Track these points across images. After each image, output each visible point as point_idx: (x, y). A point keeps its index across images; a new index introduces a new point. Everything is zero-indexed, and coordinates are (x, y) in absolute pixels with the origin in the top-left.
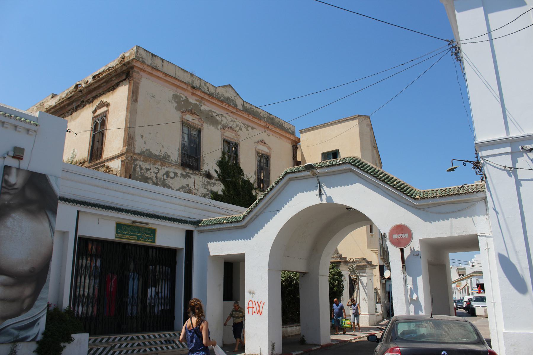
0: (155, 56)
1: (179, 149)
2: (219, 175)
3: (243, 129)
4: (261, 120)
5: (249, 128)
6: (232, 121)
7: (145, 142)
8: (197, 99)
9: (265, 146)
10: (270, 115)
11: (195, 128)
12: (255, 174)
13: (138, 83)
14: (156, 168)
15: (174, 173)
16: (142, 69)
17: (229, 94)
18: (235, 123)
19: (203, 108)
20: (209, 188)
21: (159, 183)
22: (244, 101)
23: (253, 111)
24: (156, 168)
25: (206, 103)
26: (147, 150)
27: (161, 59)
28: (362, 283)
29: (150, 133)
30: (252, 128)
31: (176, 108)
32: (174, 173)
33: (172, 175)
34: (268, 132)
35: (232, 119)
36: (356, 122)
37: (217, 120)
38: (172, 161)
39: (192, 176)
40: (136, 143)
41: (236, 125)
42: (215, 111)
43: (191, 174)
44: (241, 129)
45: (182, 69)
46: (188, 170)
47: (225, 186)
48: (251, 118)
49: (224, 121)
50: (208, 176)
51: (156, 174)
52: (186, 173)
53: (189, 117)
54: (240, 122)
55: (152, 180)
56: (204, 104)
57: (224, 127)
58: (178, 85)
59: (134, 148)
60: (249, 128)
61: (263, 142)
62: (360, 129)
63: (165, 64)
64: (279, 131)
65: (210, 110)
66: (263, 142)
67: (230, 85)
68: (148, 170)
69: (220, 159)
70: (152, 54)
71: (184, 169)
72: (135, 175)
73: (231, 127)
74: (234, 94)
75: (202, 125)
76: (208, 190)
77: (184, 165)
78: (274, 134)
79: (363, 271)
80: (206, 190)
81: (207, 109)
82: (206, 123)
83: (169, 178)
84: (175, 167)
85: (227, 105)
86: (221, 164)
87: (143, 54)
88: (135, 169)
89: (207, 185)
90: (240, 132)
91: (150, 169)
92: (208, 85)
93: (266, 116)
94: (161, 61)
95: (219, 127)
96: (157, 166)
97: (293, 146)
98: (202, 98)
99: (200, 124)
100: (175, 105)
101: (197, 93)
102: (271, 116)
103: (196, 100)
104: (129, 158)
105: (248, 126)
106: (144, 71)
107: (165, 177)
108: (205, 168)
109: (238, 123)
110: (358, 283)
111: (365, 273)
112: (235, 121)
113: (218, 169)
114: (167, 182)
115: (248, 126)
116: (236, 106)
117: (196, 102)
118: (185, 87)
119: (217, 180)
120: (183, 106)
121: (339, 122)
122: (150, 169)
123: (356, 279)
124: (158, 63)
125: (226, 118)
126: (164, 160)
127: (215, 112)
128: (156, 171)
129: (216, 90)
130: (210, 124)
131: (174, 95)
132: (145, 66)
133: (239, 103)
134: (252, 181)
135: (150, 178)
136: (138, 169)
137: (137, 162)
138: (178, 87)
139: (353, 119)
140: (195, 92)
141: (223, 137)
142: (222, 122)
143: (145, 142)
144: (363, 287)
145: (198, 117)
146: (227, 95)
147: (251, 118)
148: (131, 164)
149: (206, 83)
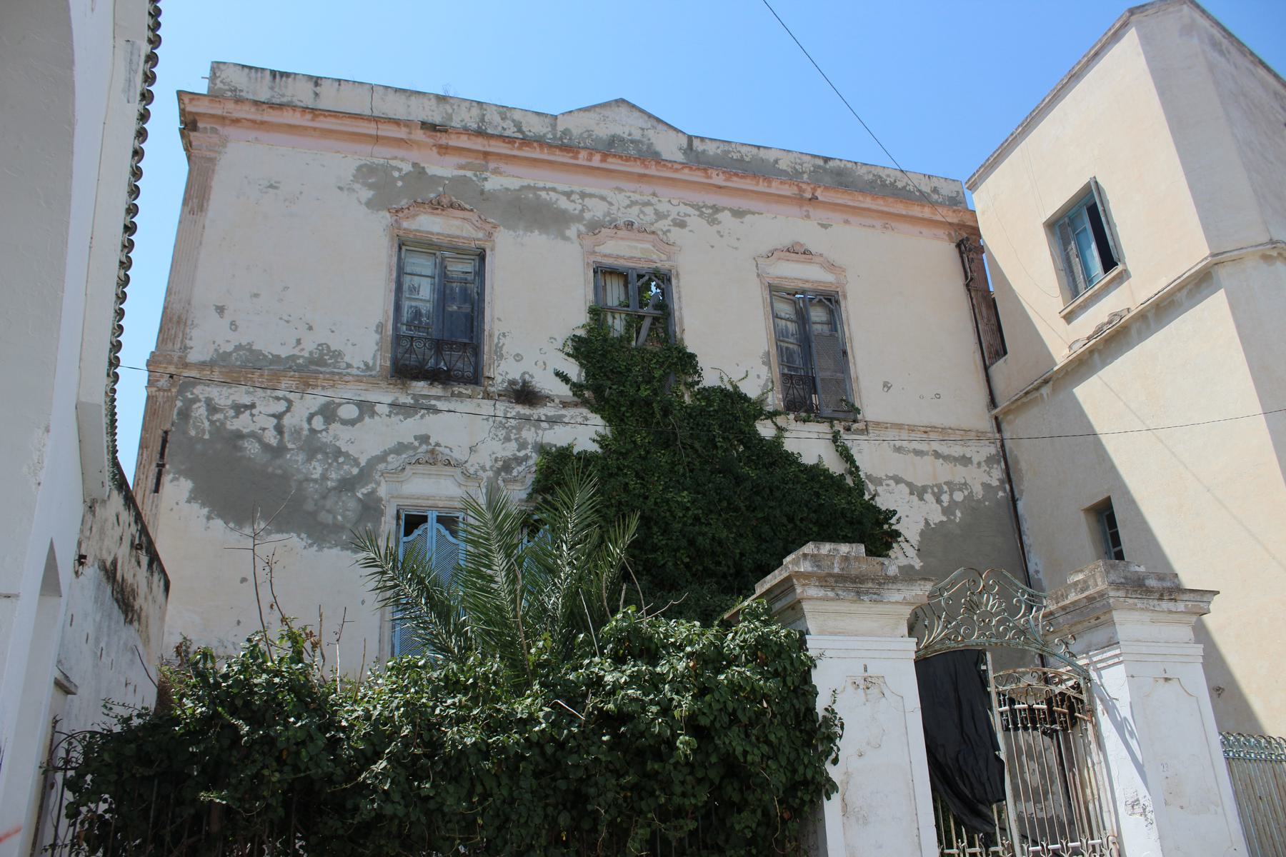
0: (287, 75)
1: (380, 328)
2: (577, 388)
3: (694, 221)
4: (768, 180)
5: (725, 216)
6: (633, 203)
7: (233, 323)
8: (463, 161)
9: (810, 262)
10: (826, 160)
11: (460, 252)
12: (767, 363)
13: (212, 161)
14: (278, 398)
15: (361, 405)
16: (223, 118)
17: (625, 125)
18: (649, 210)
19: (493, 183)
20: (529, 435)
21: (290, 446)
22: (690, 138)
23: (741, 160)
24: (278, 398)
25: (503, 167)
26: (239, 347)
27: (310, 77)
28: (1110, 709)
29: (256, 295)
30: (738, 214)
31: (369, 204)
32: (361, 405)
33: (349, 412)
34: (819, 214)
35: (635, 197)
36: (1131, 38)
37: (564, 212)
38: (349, 366)
39: (440, 405)
40: (195, 333)
41: (657, 213)
42: (549, 185)
43: (438, 398)
44: (682, 225)
45: (397, 90)
46: (420, 387)
47: (609, 421)
48: (719, 180)
49: (597, 210)
50: (525, 394)
51: (279, 416)
52: (415, 397)
53: (431, 224)
54: (671, 202)
55: (259, 439)
56: (496, 172)
57: (595, 227)
58: (374, 132)
59: (185, 348)
60: (725, 216)
61: (798, 252)
62: (1149, 61)
63: (324, 89)
64: (879, 205)
65: (523, 188)
66: (798, 252)
67: (623, 101)
68: (239, 409)
69: (582, 333)
70: (273, 73)
71: (404, 388)
72: (185, 433)
73: (630, 225)
74: (642, 122)
75: (490, 235)
76: (522, 446)
77: (403, 371)
78: (852, 219)
79: (1100, 636)
80: (514, 445)
81: (513, 183)
82: (509, 228)
83: (335, 426)
84: (363, 386)
85: (597, 157)
86: (590, 348)
87: (240, 80)
88: (185, 414)
89: (519, 429)
90: (676, 234)
91: (253, 406)
92: (517, 116)
93: (808, 166)
94: (310, 85)
95: (572, 232)
96: (280, 394)
97: (958, 246)
98: (486, 155)
99: (481, 235)
100: (367, 194)
101: (451, 143)
102: (831, 164)
103: (461, 167)
104: (164, 382)
105: (716, 209)
106: (236, 121)
107: (318, 423)
108: (504, 371)
109: (663, 207)
110: (1092, 712)
111: (1112, 643)
112: (648, 204)
113: (574, 370)
114: (325, 438)
115: (716, 209)
116: (656, 158)
117: (462, 172)
118: (401, 133)
119: (565, 405)
120: (385, 191)
121: (1074, 77)
122: (253, 406)
123: (1077, 687)
124: (303, 94)
125: (603, 198)
126: (312, 370)
127: (554, 190)
128: (281, 406)
129: (554, 126)
130: (529, 228)
131: (359, 169)
132: (230, 106)
133: (669, 148)
134: (751, 390)
135: (253, 435)
136: (200, 411)
137: (198, 390)
138: (377, 139)
139: (1116, 36)
141: (592, 259)
142: (587, 215)
143: (233, 323)
144: (1120, 726)
145: (467, 215)
146: (603, 131)
147: (719, 180)
148: (172, 401)
149: (504, 111)
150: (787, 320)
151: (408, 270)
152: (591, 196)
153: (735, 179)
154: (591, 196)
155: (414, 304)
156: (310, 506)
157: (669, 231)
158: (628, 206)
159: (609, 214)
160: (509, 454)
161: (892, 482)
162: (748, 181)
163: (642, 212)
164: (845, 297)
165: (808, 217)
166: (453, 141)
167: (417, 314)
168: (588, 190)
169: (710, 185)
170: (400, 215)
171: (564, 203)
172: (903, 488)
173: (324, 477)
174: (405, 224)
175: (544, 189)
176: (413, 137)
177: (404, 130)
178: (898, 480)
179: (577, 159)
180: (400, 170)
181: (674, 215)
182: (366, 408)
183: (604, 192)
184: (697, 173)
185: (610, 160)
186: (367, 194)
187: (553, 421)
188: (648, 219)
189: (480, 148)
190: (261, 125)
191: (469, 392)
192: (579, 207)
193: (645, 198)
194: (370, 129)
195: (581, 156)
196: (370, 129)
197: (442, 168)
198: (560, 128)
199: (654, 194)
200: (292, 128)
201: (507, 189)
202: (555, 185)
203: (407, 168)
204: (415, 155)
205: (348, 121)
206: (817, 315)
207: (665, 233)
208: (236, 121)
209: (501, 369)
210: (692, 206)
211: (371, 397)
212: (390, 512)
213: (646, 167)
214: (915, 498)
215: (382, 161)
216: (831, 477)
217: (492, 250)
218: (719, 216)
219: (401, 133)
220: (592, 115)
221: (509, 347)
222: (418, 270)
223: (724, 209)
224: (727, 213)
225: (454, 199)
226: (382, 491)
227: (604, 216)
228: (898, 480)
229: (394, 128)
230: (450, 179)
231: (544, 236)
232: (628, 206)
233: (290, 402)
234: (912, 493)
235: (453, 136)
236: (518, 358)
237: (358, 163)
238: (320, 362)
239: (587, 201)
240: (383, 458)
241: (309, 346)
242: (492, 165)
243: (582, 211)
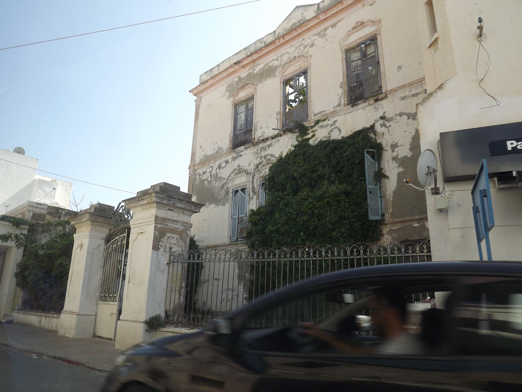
0: (213, 68)
3: (319, 41)
19: (257, 69)
20: (263, 154)
22: (319, 4)
30: (333, 26)
33: (223, 165)
35: (297, 45)
42: (269, 61)
44: (312, 45)
49: (285, 58)
58: (227, 74)
60: (330, 31)
61: (361, 25)
66: (361, 25)
76: (261, 158)
80: (259, 158)
81: (261, 66)
85: (281, 39)
90: (311, 51)
98: (254, 61)
101: (244, 64)
103: (249, 70)
105: (325, 30)
106: (202, 91)
109: (306, 43)
118: (232, 70)
127: (273, 60)
149: (260, 41)
152: (284, 54)
153: (329, 12)
154: (284, 54)
156: (216, 196)
158: (295, 50)
160: (258, 162)
161: (398, 117)
162: (334, 9)
163: (300, 50)
164: (380, 34)
165: (364, 5)
166: (245, 63)
167: (241, 125)
168: (283, 53)
169: (321, 21)
171: (276, 63)
172: (405, 117)
173: (219, 186)
174: (236, 99)
175: (271, 61)
176: (235, 69)
178: (401, 115)
179: (276, 44)
181: (310, 43)
182: (227, 162)
183: (287, 50)
184: (314, 20)
185: (285, 37)
186: (228, 94)
187: (269, 146)
188: (301, 51)
190: (207, 88)
193: (300, 43)
194: (225, 74)
196: (225, 74)
198: (277, 34)
199: (303, 39)
200: (212, 85)
203: (236, 79)
205: (221, 75)
206: (370, 50)
207: (307, 53)
208: (202, 91)
211: (228, 158)
212: (231, 191)
213: (297, 31)
214: (411, 120)
217: (256, 93)
218: (327, 32)
219: (232, 70)
220: (287, 21)
221: (259, 125)
222: (241, 111)
223: (328, 27)
224: (330, 28)
226: (229, 187)
228: (401, 115)
229: (230, 69)
232: (295, 50)
233: (212, 167)
234: (409, 118)
237: (225, 86)
238: (217, 153)
240: (229, 176)
241: (216, 149)
242: (256, 63)
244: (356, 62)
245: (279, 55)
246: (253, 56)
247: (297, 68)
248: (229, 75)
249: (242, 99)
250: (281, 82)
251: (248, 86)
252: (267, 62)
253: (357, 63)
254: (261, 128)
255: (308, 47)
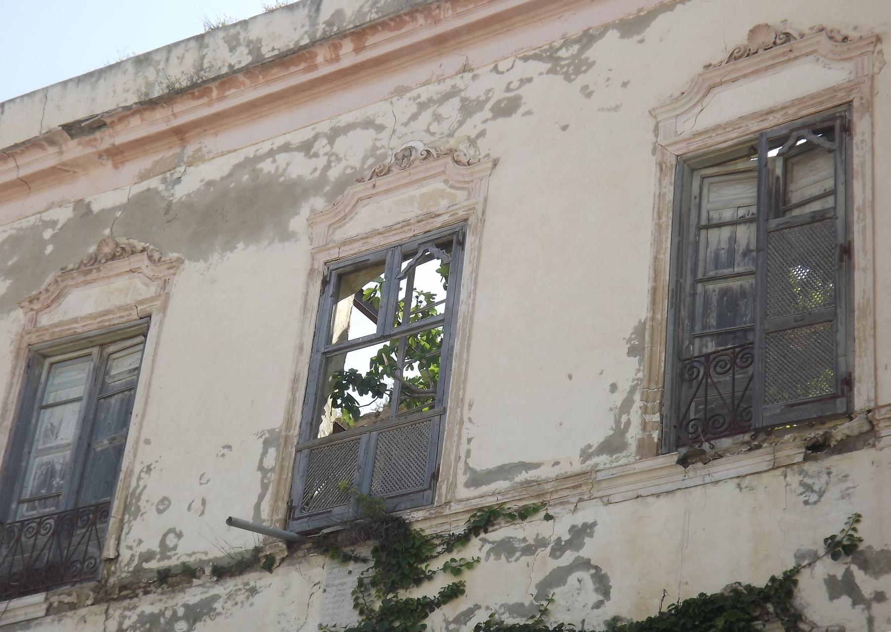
3: (545, 90)
5: (609, 50)
9: (791, 58)
19: (192, 181)
35: (425, 93)
42: (266, 147)
44: (507, 108)
49: (354, 150)
60: (609, 50)
73: (405, 157)
81: (213, 170)
85: (348, 46)
98: (180, 133)
101: (120, 140)
103: (144, 176)
105: (588, 38)
109: (474, 91)
118: (47, 159)
125: (369, 124)
127: (286, 148)
140: (106, 140)
141: (323, 257)
149: (232, 33)
150: (734, 223)
151: (50, 399)
155: (46, 459)
157: (482, 134)
158: (414, 117)
159: (375, 148)
163: (437, 118)
164: (869, 107)
167: (50, 473)
168: (345, 120)
170: (37, 306)
171: (299, 167)
174: (45, 320)
175: (271, 153)
176: (67, 157)
177: (51, 150)
179: (313, 67)
180: (53, 223)
181: (499, 94)
183: (370, 111)
185: (370, 40)
188: (445, 127)
189: (163, 127)
191: (72, 599)
192: (322, 161)
193: (446, 87)
195: (320, 59)
197: (111, 190)
199: (465, 69)
201: (210, 183)
202: (288, 138)
203: (64, 215)
204: (77, 188)
206: (811, 181)
207: (472, 142)
209: (129, 539)
210: (536, 57)
213: (437, 21)
215: (32, 219)
216: (761, 591)
217: (164, 308)
218: (594, 52)
219: (47, 159)
221: (152, 489)
222: (63, 395)
223: (606, 28)
224: (613, 35)
225: (123, 241)
227: (364, 161)
230: (122, 207)
231: (252, 248)
232: (414, 117)
235: (119, 128)
236: (164, 505)
239: (341, 144)
242: (190, 149)
243: (328, 167)
244: (726, 232)
245: (325, 127)
246: (178, 108)
247: (413, 212)
248: (26, 184)
249: (79, 328)
250: (311, 272)
251: (122, 265)
252: (250, 152)
253: (733, 240)
254: (164, 505)
255: (487, 113)
